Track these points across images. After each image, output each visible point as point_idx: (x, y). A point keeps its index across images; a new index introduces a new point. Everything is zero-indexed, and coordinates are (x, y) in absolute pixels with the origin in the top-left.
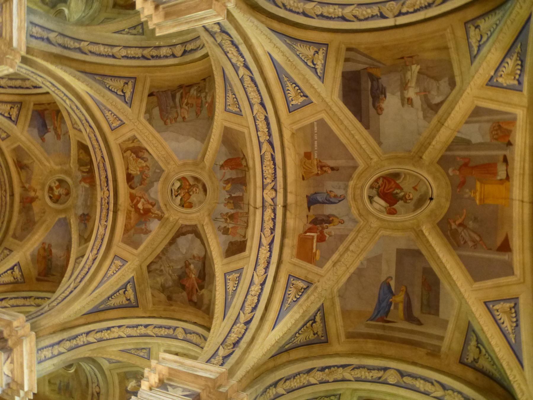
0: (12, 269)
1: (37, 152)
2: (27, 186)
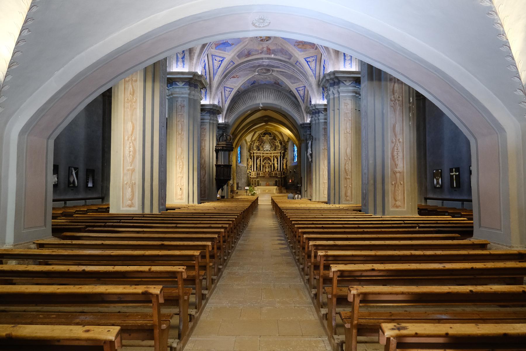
0: (307, 62)
1: (240, 48)
2: (260, 51)
